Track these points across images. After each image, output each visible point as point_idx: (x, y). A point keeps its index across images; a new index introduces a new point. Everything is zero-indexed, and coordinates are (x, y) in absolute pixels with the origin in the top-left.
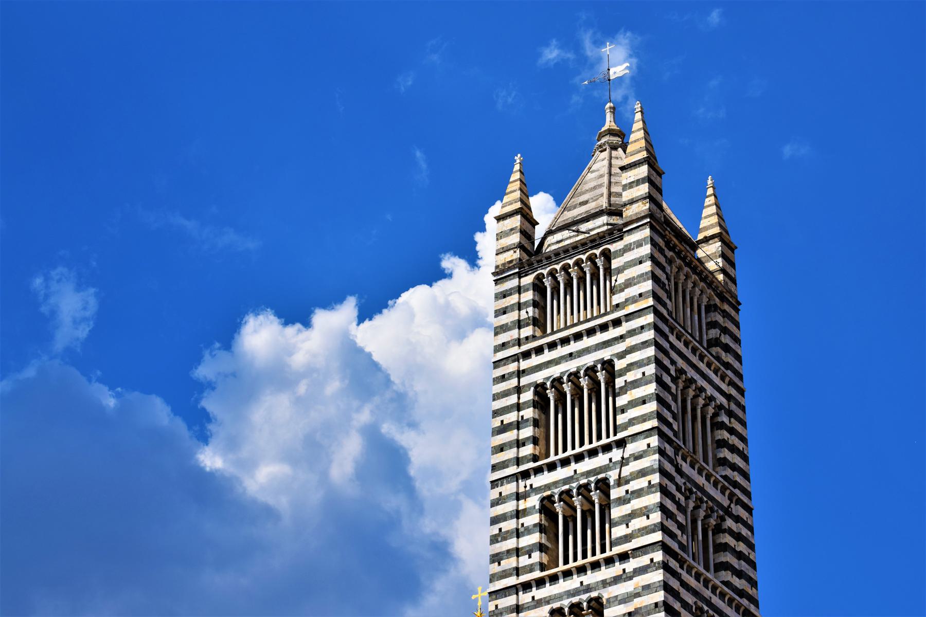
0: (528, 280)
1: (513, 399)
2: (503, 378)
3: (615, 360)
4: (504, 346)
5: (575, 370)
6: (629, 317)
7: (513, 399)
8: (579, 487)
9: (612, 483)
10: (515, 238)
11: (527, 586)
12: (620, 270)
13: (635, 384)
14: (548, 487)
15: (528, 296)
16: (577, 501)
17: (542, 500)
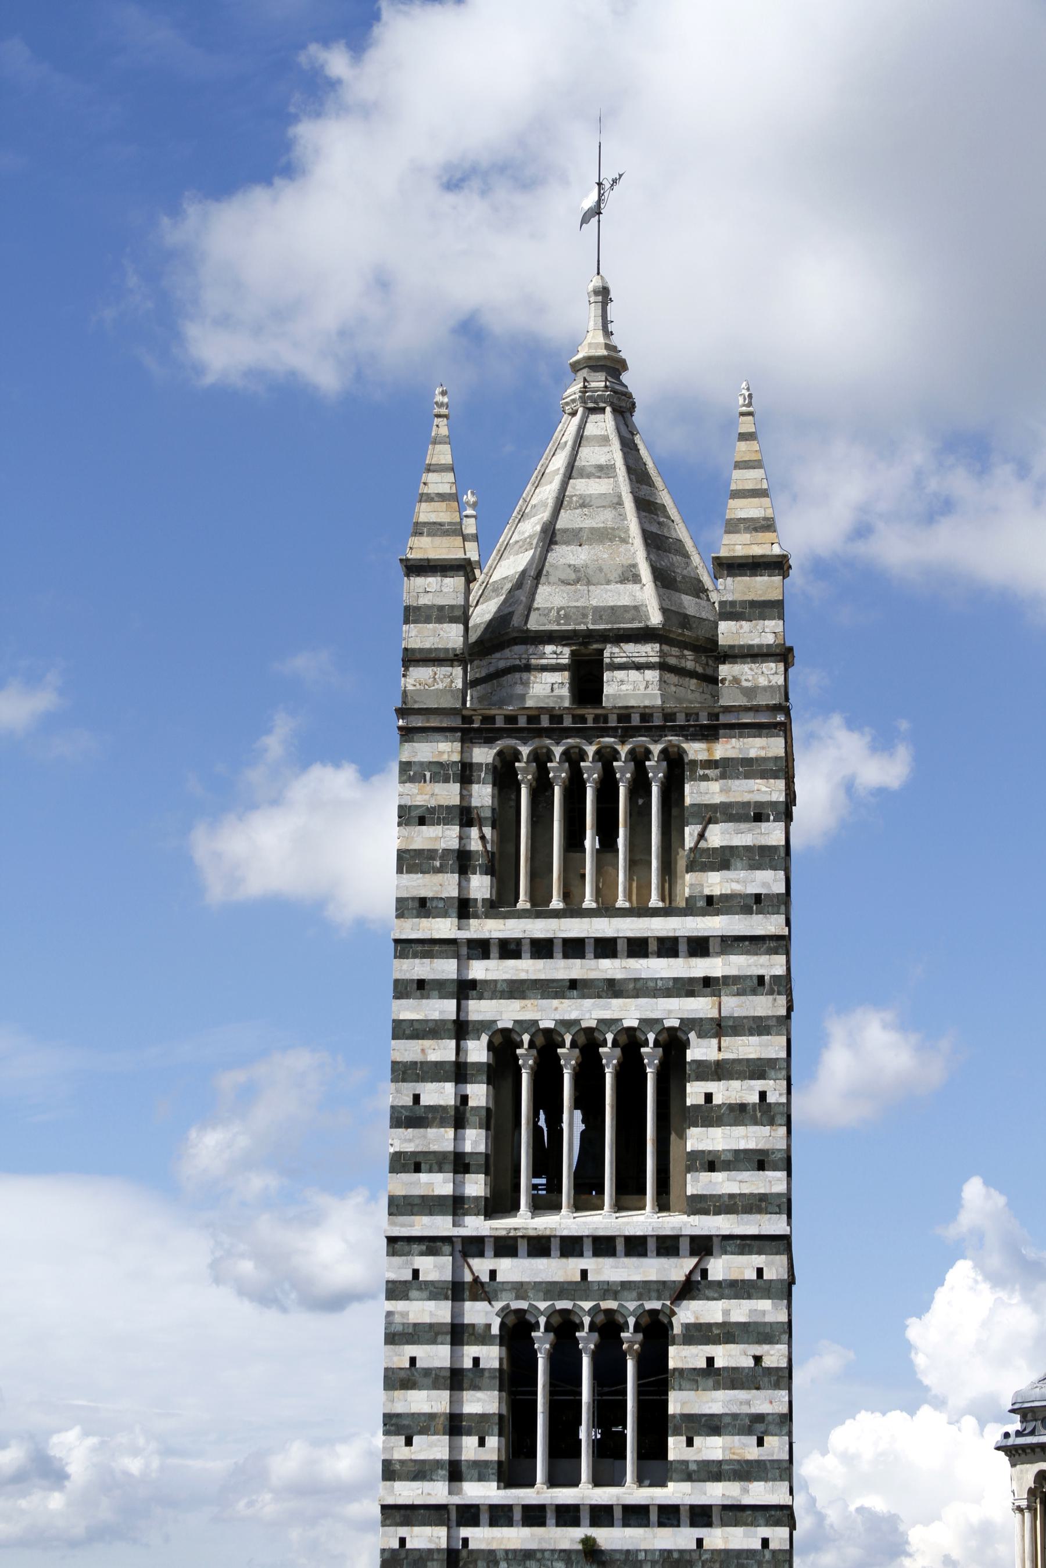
0: (483, 755)
1: (443, 1051)
2: (422, 987)
3: (692, 1036)
4: (423, 907)
5: (593, 1024)
6: (731, 944)
7: (443, 1051)
8: (595, 1311)
9: (677, 1330)
10: (451, 636)
11: (469, 1515)
12: (710, 814)
13: (739, 1114)
14: (520, 1289)
15: (483, 795)
16: (586, 1340)
17: (505, 1313)
